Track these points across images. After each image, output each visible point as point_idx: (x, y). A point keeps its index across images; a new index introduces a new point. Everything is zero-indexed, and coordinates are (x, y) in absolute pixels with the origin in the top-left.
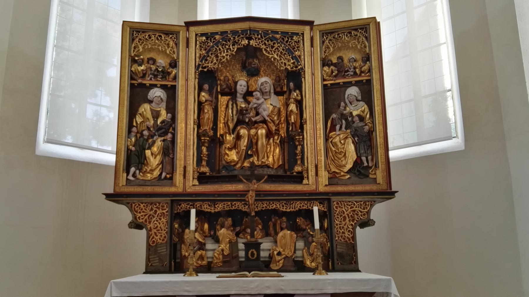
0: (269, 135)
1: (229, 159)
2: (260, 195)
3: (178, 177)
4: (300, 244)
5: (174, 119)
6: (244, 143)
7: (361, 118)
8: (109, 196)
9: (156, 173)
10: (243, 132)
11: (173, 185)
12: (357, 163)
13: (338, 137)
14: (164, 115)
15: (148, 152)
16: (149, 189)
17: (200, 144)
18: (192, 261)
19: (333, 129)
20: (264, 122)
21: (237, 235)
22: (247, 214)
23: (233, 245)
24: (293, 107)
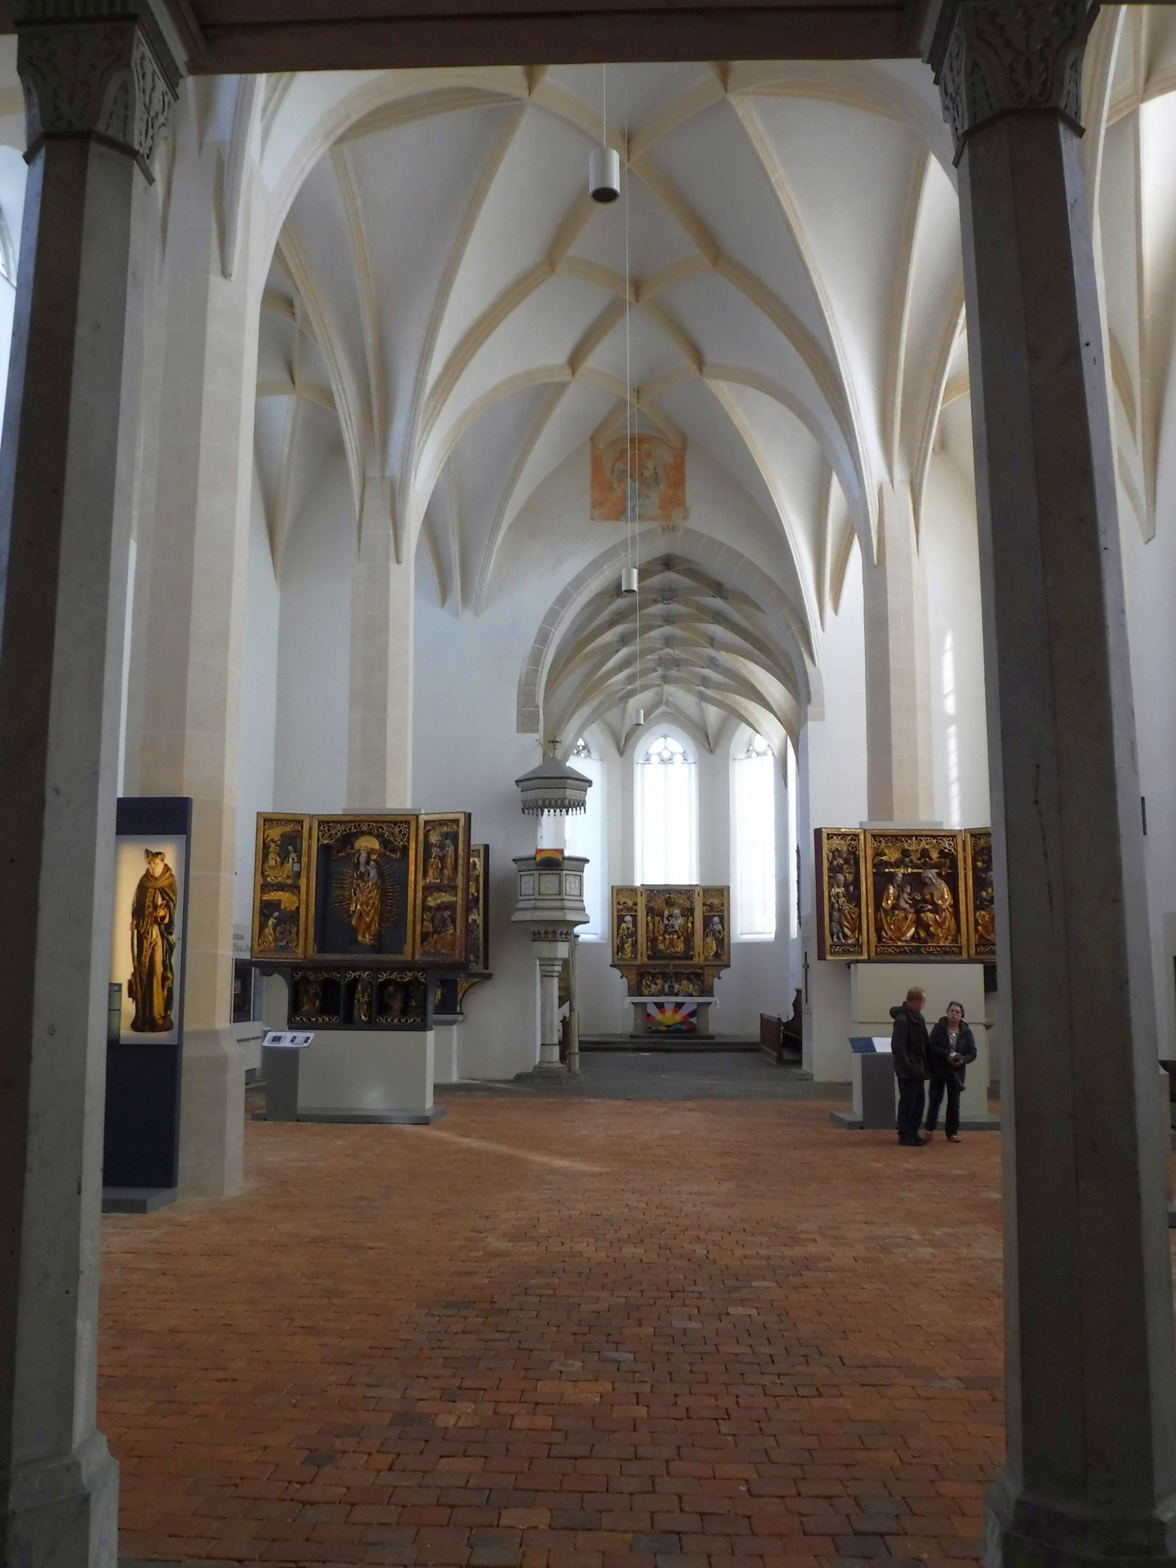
0: (679, 937)
1: (660, 948)
2: (674, 966)
3: (639, 957)
4: (691, 986)
5: (636, 930)
6: (667, 942)
7: (719, 932)
8: (611, 966)
9: (629, 955)
10: (667, 936)
11: (637, 960)
12: (717, 952)
13: (709, 940)
14: (632, 929)
15: (626, 946)
16: (626, 963)
17: (647, 941)
18: (646, 992)
19: (707, 936)
20: (676, 931)
21: (664, 982)
22: (669, 973)
23: (663, 987)
24: (690, 925)
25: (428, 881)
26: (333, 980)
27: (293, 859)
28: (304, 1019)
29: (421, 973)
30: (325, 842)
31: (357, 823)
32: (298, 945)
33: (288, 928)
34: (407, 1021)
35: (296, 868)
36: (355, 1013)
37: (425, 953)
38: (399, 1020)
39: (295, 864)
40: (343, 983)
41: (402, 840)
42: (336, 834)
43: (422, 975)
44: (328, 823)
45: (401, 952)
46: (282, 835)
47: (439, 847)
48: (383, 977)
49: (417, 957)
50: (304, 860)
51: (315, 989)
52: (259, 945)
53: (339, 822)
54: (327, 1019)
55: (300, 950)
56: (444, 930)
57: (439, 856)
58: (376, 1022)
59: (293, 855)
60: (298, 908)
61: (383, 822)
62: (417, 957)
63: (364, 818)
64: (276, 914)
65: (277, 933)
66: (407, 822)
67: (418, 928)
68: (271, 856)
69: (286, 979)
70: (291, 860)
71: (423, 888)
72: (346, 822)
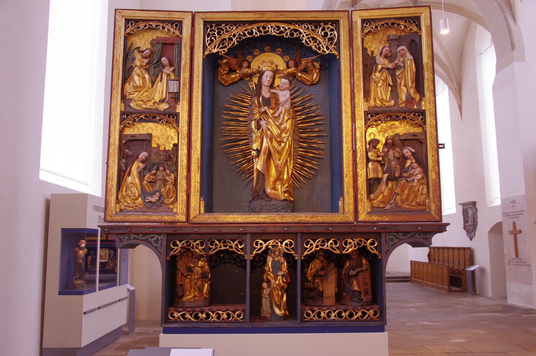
25: (372, 103)
26: (233, 252)
27: (168, 75)
28: (188, 316)
29: (370, 241)
30: (215, 51)
31: (262, 24)
32: (176, 200)
33: (160, 175)
34: (351, 315)
35: (173, 87)
36: (265, 303)
37: (374, 210)
38: (339, 315)
39: (171, 82)
40: (249, 257)
41: (328, 49)
42: (231, 39)
43: (371, 244)
44: (218, 23)
45: (334, 209)
46: (153, 43)
47: (386, 57)
48: (314, 246)
49: (362, 217)
50: (185, 75)
51: (202, 267)
52: (118, 201)
53: (236, 23)
54: (225, 316)
55: (180, 208)
56: (404, 175)
57: (388, 69)
58: (303, 320)
59: (168, 70)
60: (176, 146)
61: (300, 23)
62: (362, 217)
63: (272, 17)
64: (143, 155)
65: (145, 182)
66: (336, 23)
67: (361, 172)
68: (137, 70)
69: (159, 253)
70: (165, 77)
71: (366, 113)
72: (244, 23)
